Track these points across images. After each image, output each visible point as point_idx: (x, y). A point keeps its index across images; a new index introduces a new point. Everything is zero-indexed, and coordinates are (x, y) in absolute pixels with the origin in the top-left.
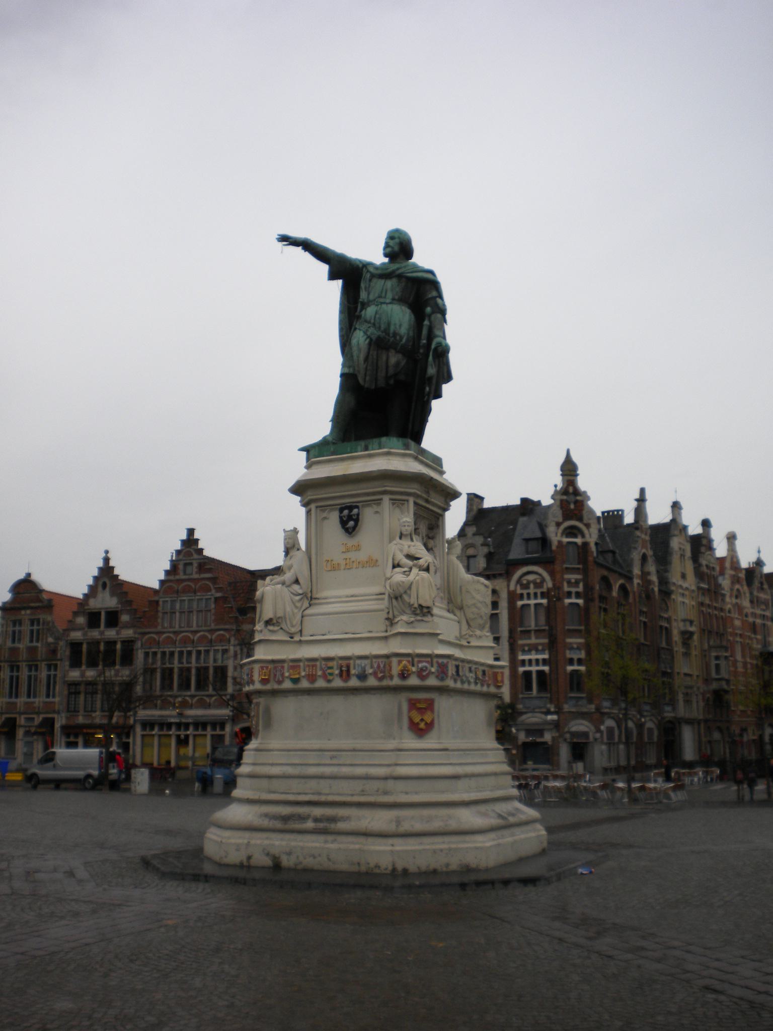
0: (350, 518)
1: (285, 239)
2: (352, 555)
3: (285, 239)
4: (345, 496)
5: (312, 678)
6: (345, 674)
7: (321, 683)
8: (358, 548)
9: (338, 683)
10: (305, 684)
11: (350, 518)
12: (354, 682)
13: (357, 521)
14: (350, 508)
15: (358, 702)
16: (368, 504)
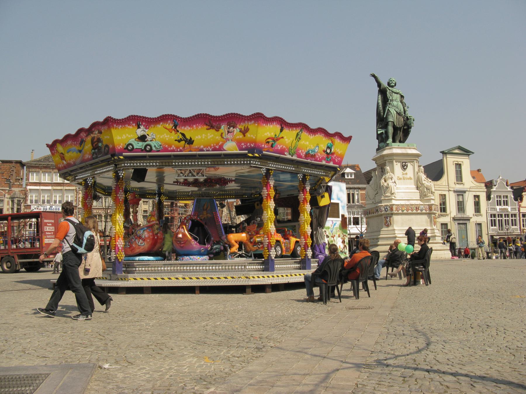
0: (405, 165)
1: (374, 76)
2: (405, 176)
3: (374, 76)
4: (404, 159)
5: (407, 210)
6: (417, 209)
7: (410, 211)
8: (406, 174)
9: (415, 211)
10: (405, 212)
11: (405, 165)
12: (419, 211)
13: (407, 166)
14: (405, 163)
15: (418, 216)
16: (410, 162)
